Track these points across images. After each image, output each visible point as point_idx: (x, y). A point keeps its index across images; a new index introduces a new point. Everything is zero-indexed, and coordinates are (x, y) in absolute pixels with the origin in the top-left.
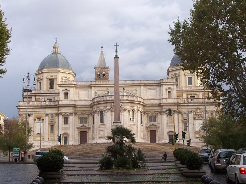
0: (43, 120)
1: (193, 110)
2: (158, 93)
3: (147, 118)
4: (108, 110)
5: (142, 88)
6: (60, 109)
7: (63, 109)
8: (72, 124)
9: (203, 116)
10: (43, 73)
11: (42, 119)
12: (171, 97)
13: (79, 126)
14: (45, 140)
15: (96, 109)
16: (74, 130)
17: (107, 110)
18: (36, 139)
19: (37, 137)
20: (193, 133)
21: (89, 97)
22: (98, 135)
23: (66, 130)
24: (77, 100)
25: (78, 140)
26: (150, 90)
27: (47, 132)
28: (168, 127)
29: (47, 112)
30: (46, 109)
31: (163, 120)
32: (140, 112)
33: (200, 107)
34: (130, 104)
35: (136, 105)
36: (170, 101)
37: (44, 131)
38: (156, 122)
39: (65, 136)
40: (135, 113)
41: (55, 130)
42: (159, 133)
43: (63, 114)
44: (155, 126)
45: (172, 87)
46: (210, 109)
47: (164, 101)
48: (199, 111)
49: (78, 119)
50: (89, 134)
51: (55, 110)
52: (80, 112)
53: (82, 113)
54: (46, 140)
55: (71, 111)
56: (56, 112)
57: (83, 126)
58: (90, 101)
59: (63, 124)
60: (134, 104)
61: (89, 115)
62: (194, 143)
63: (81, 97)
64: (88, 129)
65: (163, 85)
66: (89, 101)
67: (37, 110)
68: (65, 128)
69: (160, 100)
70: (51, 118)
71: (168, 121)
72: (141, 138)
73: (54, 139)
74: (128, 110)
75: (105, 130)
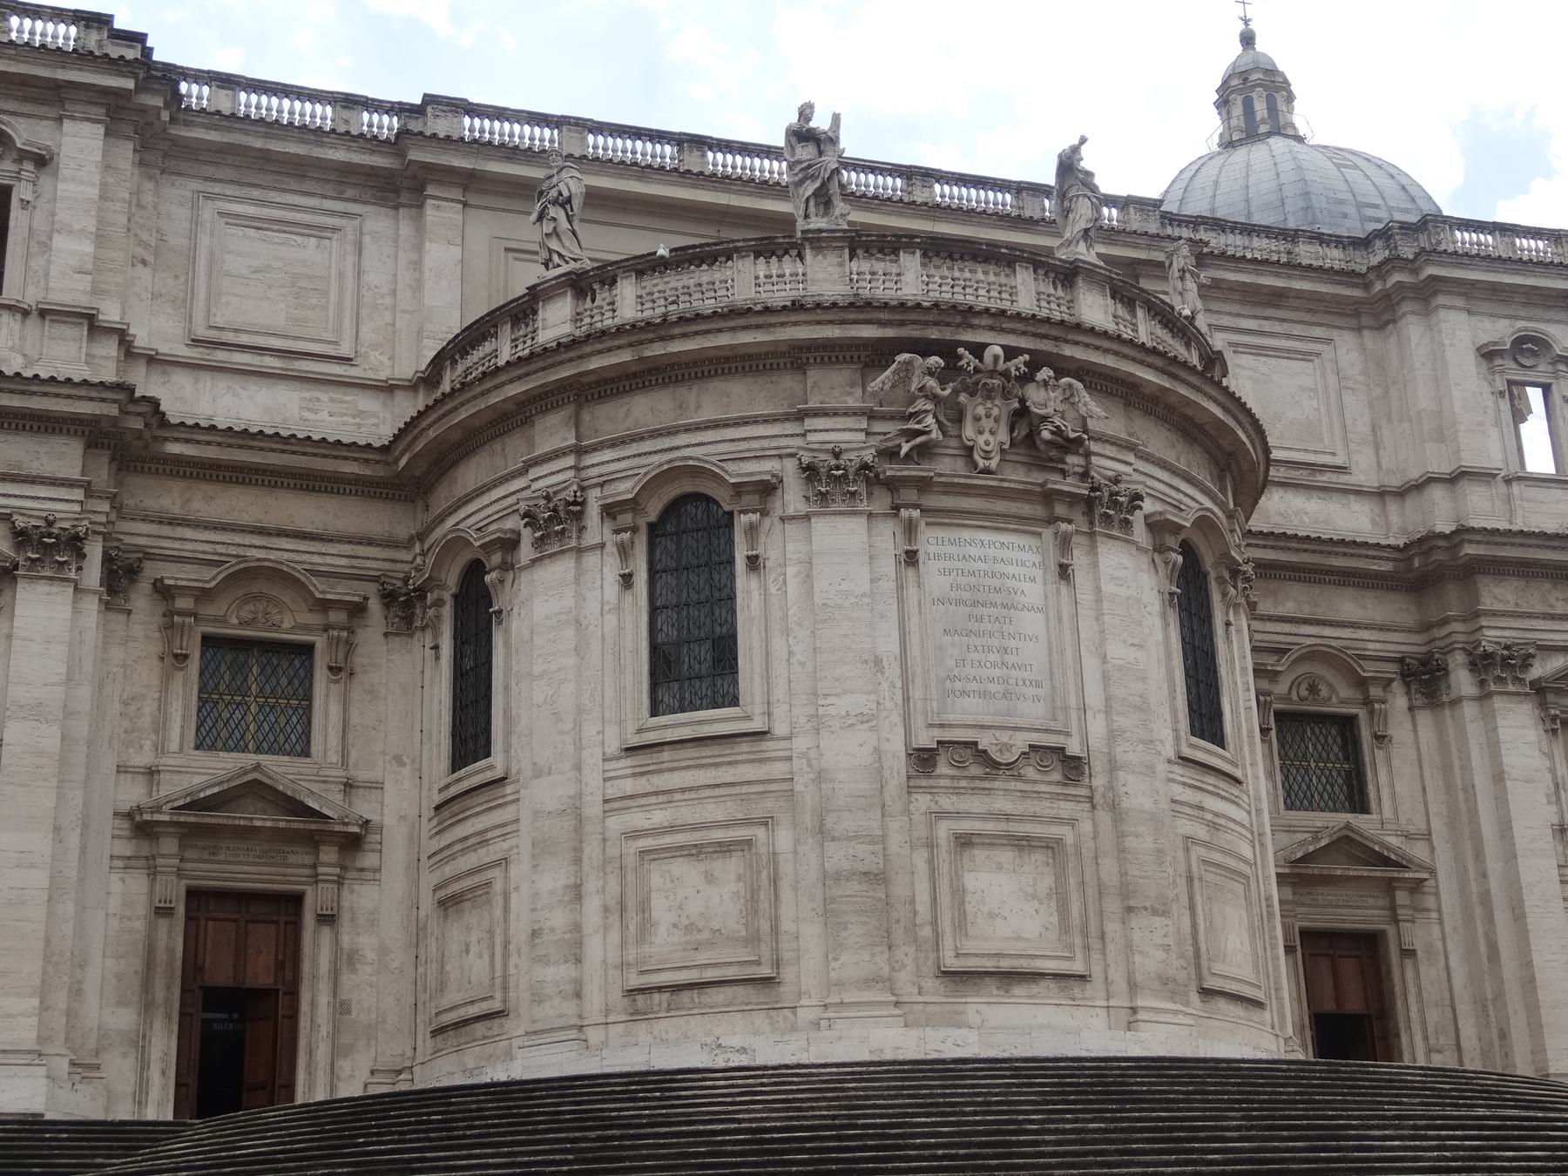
2: (1357, 409)
8: (50, 738)
13: (174, 787)
15: (554, 476)
16: (83, 850)
17: (810, 472)
21: (367, 333)
24: (163, 349)
25: (139, 1043)
31: (1499, 777)
34: (1158, 440)
42: (1430, 973)
44: (1386, 862)
49: (148, 674)
50: (346, 940)
52: (196, 542)
53: (247, 576)
55: (63, 507)
57: (256, 790)
58: (387, 388)
61: (357, 610)
63: (220, 321)
64: (329, 854)
65: (1441, 299)
66: (368, 403)
69: (1393, 506)
74: (1156, 526)
75: (784, 839)
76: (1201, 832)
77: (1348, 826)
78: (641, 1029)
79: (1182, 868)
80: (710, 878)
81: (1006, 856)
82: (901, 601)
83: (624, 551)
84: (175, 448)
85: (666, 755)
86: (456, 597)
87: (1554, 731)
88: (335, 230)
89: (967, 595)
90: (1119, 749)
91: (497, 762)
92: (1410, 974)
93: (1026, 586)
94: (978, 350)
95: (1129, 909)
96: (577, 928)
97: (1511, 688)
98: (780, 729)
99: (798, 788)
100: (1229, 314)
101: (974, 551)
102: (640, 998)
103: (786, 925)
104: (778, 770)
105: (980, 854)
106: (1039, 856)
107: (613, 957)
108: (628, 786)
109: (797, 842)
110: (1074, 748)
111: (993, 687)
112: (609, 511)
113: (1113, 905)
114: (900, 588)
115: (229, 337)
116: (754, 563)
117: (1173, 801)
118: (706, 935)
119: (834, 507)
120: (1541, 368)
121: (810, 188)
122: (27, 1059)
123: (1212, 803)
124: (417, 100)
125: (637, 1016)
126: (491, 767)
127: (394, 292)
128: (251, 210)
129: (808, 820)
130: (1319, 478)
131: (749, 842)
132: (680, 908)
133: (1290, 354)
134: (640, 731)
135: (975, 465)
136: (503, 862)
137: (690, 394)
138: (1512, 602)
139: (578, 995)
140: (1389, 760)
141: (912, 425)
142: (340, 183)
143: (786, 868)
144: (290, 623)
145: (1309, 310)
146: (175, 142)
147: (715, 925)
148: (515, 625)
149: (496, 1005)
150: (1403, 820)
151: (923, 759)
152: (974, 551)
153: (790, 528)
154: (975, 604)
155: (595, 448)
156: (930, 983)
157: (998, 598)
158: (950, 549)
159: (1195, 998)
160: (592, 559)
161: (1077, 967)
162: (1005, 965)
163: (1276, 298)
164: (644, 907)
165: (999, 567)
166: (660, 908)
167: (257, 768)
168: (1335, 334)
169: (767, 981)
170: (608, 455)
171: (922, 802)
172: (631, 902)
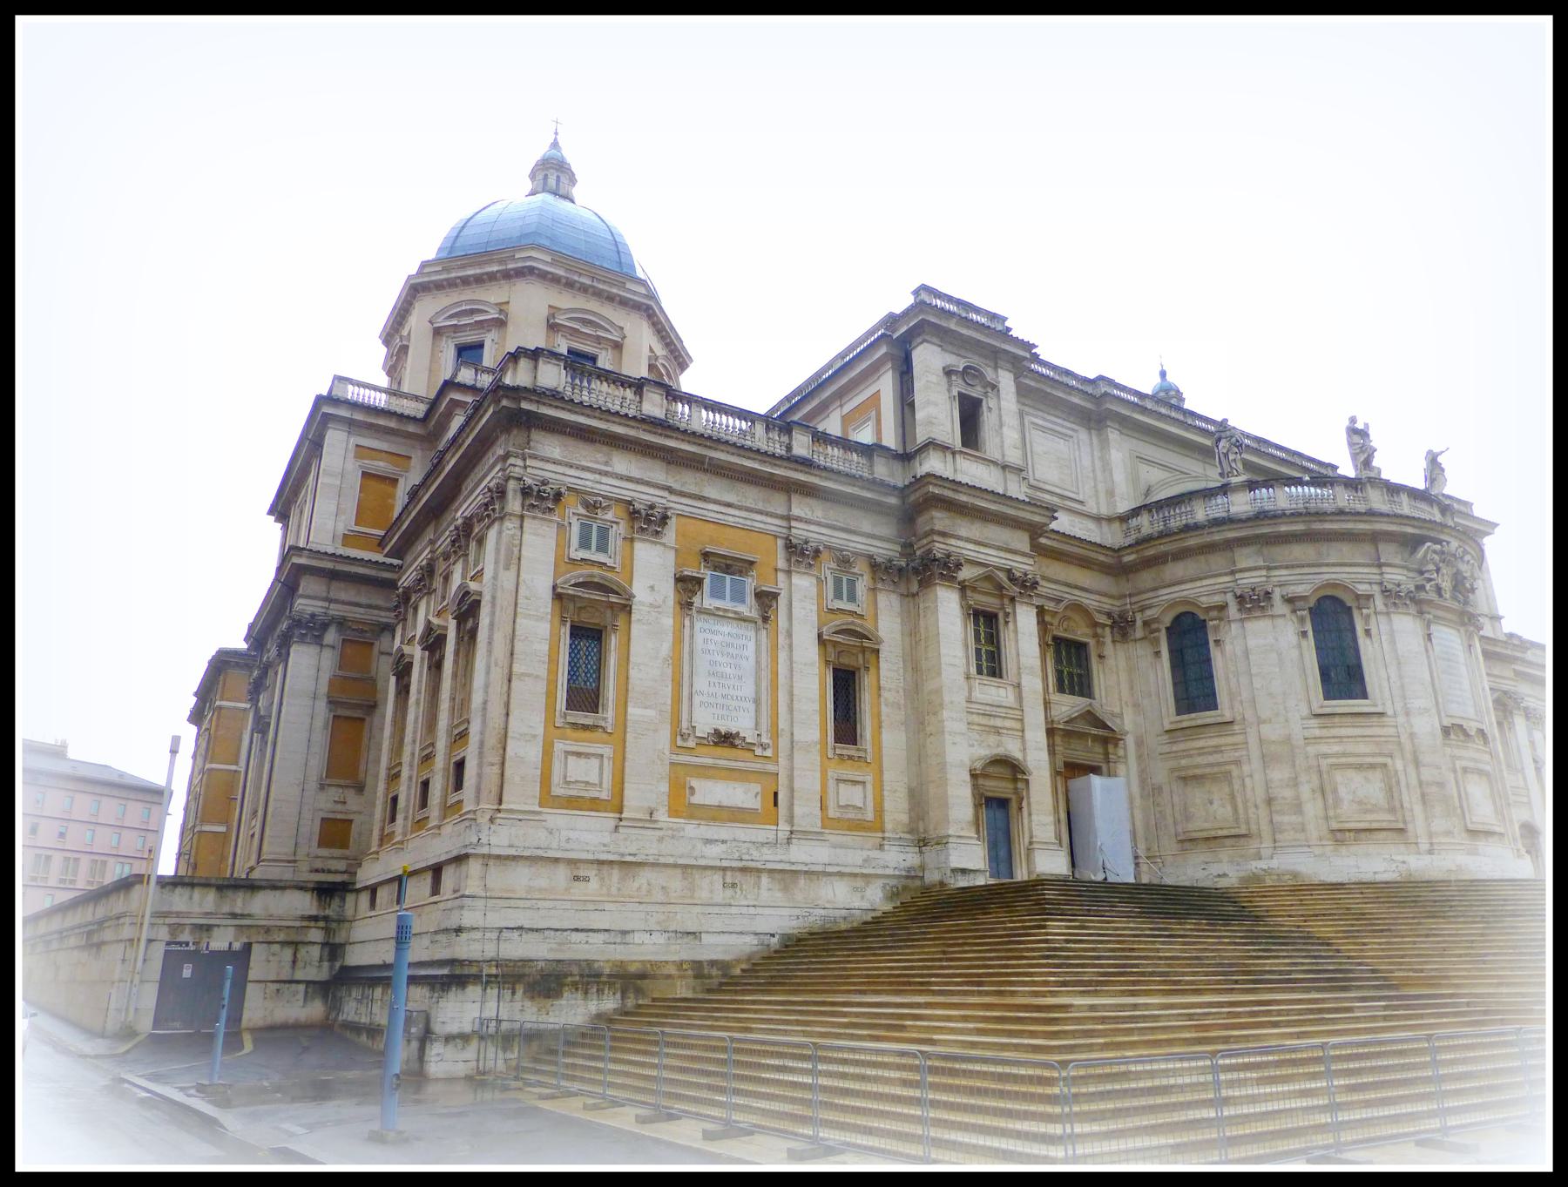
0: (766, 599)
4: (1393, 596)
6: (939, 519)
10: (520, 273)
14: (791, 819)
17: (1386, 592)
18: (696, 799)
19: (706, 772)
22: (1313, 809)
23: (997, 731)
27: (815, 735)
29: (800, 531)
30: (795, 499)
37: (783, 724)
39: (998, 787)
41: (879, 727)
43: (966, 573)
51: (866, 524)
54: (798, 810)
56: (885, 550)
59: (973, 670)
63: (1037, 476)
66: (1091, 525)
68: (992, 710)
70: (838, 595)
73: (870, 816)
75: (1399, 765)
78: (1343, 850)
80: (1366, 779)
82: (1428, 657)
83: (1302, 620)
85: (1337, 719)
86: (1168, 629)
88: (1071, 437)
91: (1225, 711)
94: (1448, 543)
96: (1298, 798)
98: (1390, 712)
99: (1402, 741)
102: (1338, 834)
103: (1406, 805)
104: (1392, 731)
107: (1321, 813)
108: (1317, 732)
109: (1405, 767)
112: (1290, 600)
114: (1427, 651)
115: (1041, 485)
116: (1368, 632)
118: (1369, 807)
119: (1400, 611)
121: (1362, 458)
122: (1052, 847)
124: (1092, 376)
125: (1339, 842)
126: (1222, 716)
127: (1094, 471)
128: (1040, 422)
129: (1408, 756)
131: (1385, 765)
132: (1354, 792)
134: (1322, 707)
135: (1440, 595)
136: (1237, 763)
137: (1324, 547)
139: (1303, 830)
141: (1426, 575)
142: (1069, 414)
143: (1402, 778)
144: (1081, 633)
147: (1373, 801)
148: (1228, 648)
149: (1243, 831)
151: (1446, 731)
153: (1382, 619)
155: (1276, 568)
156: (1464, 835)
160: (1280, 621)
161: (1502, 831)
164: (1335, 791)
166: (1342, 791)
167: (1090, 705)
169: (1401, 831)
170: (1284, 572)
171: (1448, 751)
172: (1328, 789)
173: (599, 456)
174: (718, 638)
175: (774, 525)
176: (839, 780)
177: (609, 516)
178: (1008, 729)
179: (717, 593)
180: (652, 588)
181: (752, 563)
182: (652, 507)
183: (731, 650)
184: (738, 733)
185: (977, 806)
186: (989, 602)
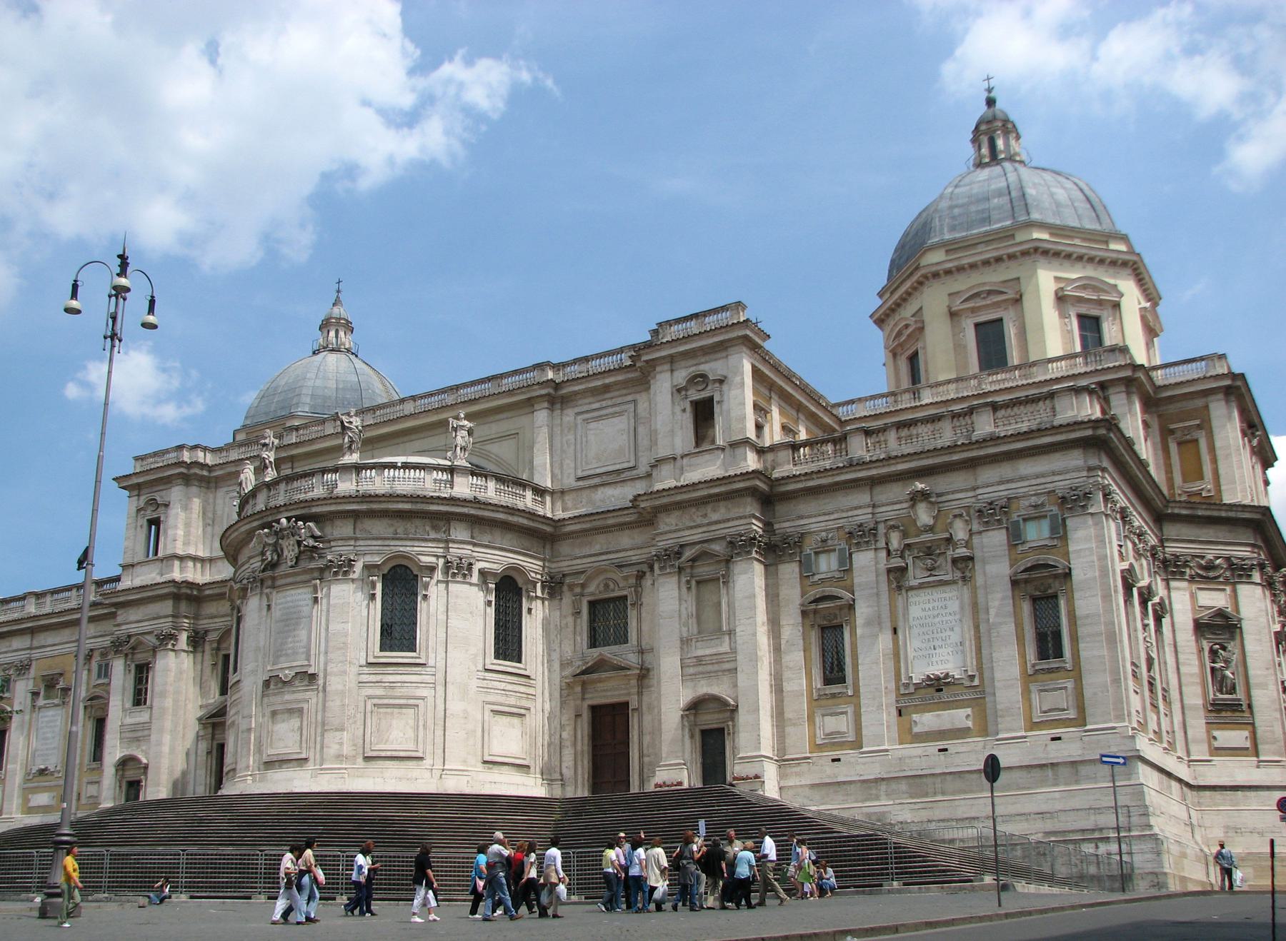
1: (887, 512)
3: (570, 620)
5: (542, 416)
6: (122, 616)
7: (134, 614)
9: (962, 551)
11: (61, 685)
12: (713, 442)
20: (889, 700)
26: (593, 425)
28: (694, 667)
32: (482, 573)
33: (941, 483)
35: (436, 528)
36: (709, 468)
38: (626, 641)
40: (426, 586)
42: (647, 719)
45: (713, 368)
46: (1020, 488)
47: (666, 480)
48: (924, 516)
55: (165, 625)
59: (129, 704)
60: (418, 522)
62: (894, 786)
65: (658, 369)
67: (50, 641)
70: (99, 676)
71: (693, 622)
72: (485, 762)
76: (380, 692)
77: (601, 654)
79: (362, 709)
81: (286, 716)
84: (208, 592)
87: (689, 589)
89: (285, 617)
90: (328, 668)
92: (636, 720)
93: (304, 608)
95: (326, 730)
97: (668, 570)
100: (586, 404)
101: (289, 599)
105: (279, 717)
106: (296, 715)
110: (311, 671)
111: (290, 651)
113: (319, 730)
117: (359, 683)
120: (709, 388)
123: (391, 678)
130: (623, 476)
133: (613, 415)
138: (674, 523)
140: (639, 614)
145: (624, 388)
146: (217, 477)
150: (643, 644)
152: (289, 599)
154: (287, 620)
157: (295, 616)
158: (283, 600)
159: (360, 760)
161: (303, 756)
162: (280, 758)
163: (606, 388)
165: (297, 603)
168: (637, 396)
171: (266, 700)
173: (8, 644)
174: (46, 719)
175: (72, 647)
176: (88, 783)
177: (11, 672)
178: (144, 737)
179: (47, 697)
180: (21, 703)
181: (61, 674)
182: (21, 662)
183: (51, 724)
184: (46, 769)
185: (120, 787)
186: (141, 657)
